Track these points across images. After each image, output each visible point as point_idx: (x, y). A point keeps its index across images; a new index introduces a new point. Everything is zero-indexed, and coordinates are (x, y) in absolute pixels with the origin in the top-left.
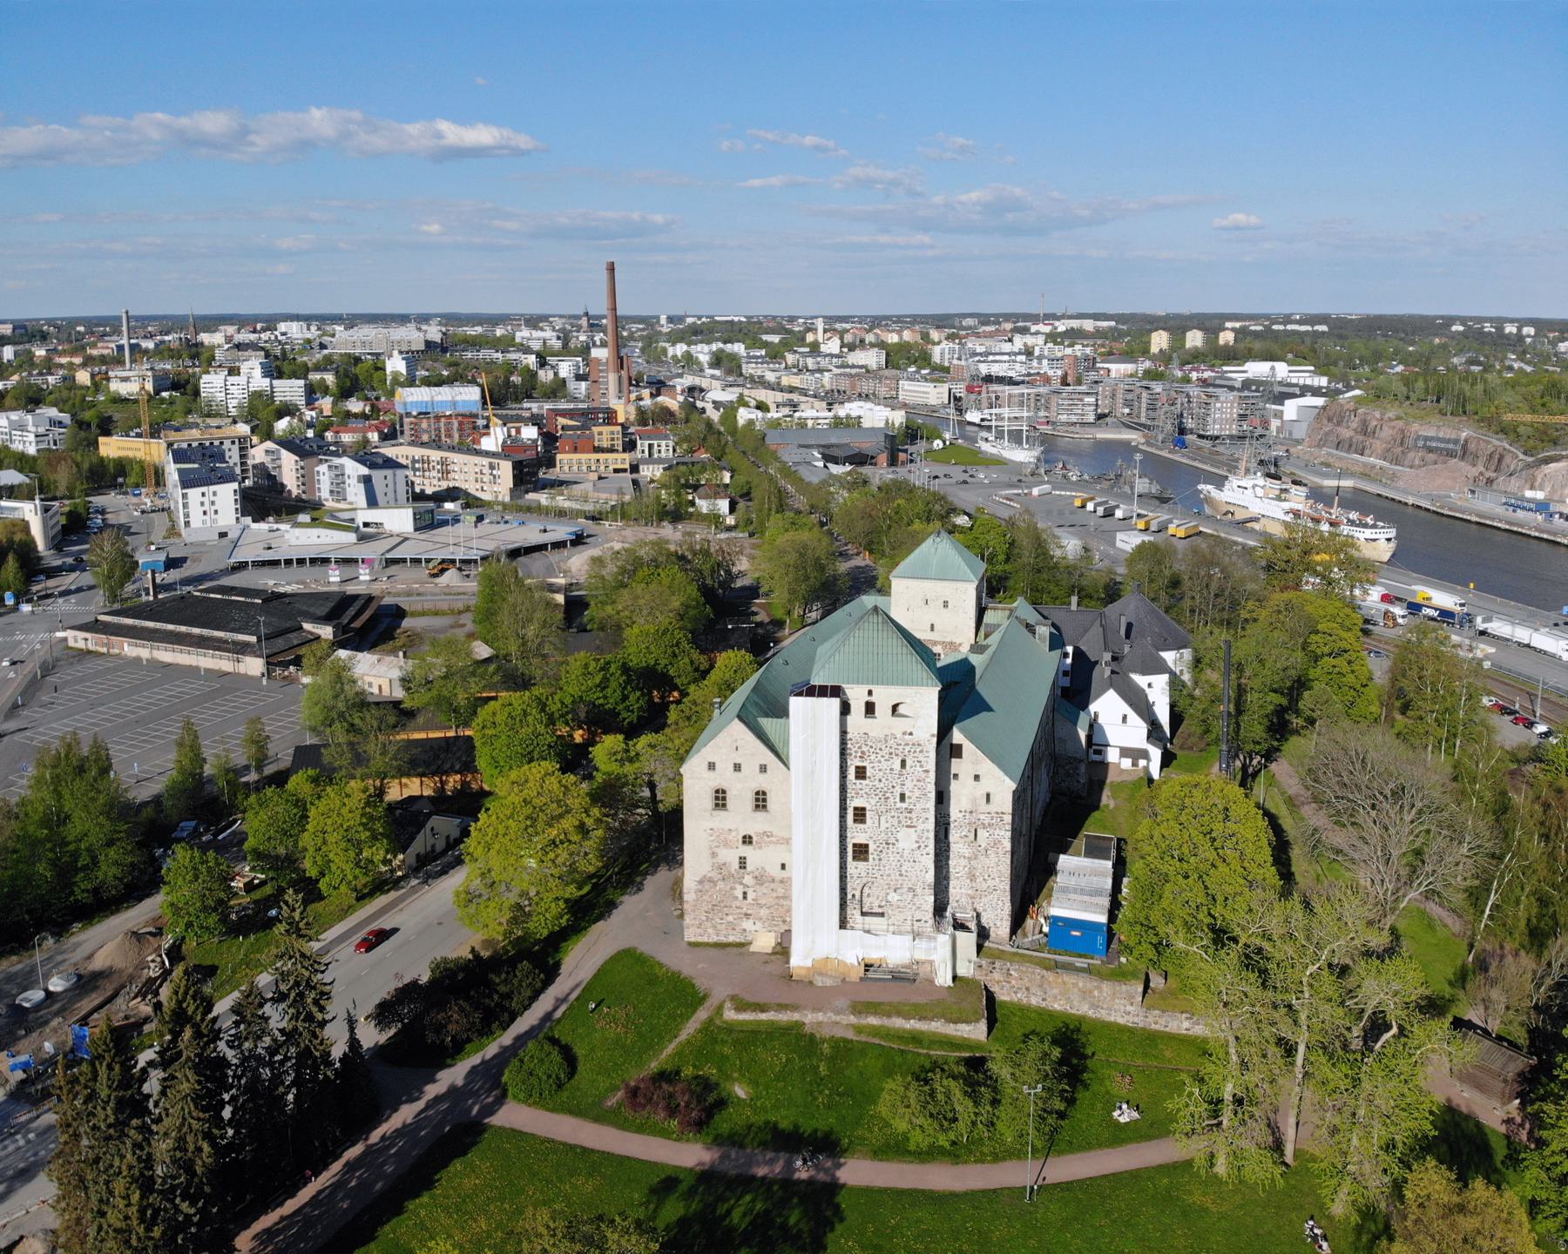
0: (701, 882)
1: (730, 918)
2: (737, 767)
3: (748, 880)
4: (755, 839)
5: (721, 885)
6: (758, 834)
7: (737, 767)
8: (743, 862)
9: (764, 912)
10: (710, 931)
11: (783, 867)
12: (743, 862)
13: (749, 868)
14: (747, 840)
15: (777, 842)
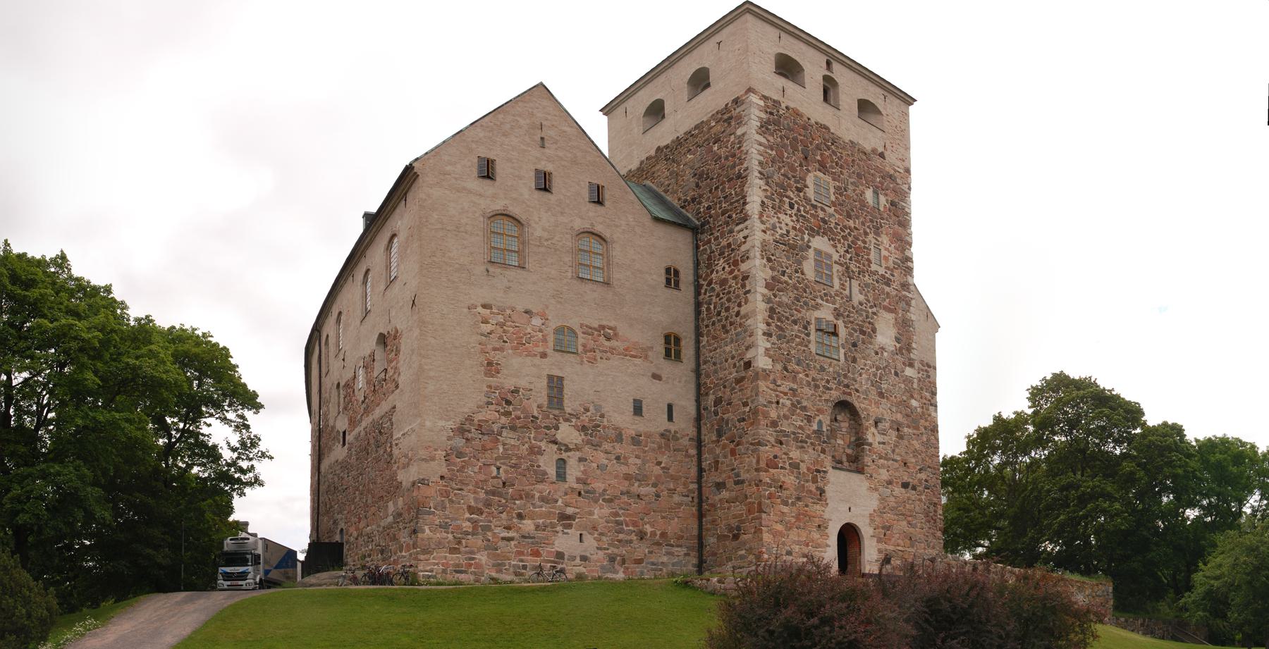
0: (461, 431)
1: (528, 525)
2: (544, 183)
3: (567, 433)
4: (581, 341)
5: (509, 437)
6: (589, 330)
7: (544, 183)
8: (556, 384)
9: (600, 513)
10: (482, 557)
11: (638, 409)
12: (556, 384)
13: (569, 406)
14: (564, 340)
15: (626, 353)
